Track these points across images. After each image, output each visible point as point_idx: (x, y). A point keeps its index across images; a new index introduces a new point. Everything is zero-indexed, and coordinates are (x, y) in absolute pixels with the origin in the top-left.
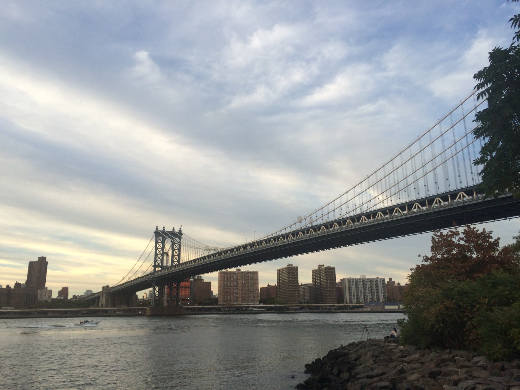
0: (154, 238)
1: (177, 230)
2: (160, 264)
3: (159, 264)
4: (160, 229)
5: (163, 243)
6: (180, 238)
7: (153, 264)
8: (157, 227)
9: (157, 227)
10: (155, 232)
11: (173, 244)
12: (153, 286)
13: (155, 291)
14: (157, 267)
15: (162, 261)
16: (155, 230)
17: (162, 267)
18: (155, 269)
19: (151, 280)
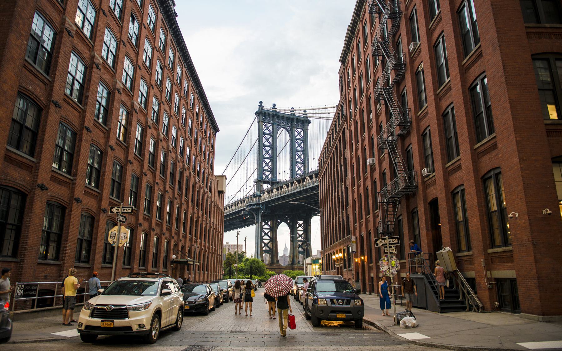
0: (256, 124)
1: (299, 113)
2: (270, 176)
3: (267, 177)
4: (268, 106)
5: (274, 135)
6: (305, 130)
7: (255, 176)
8: (261, 103)
9: (261, 103)
10: (258, 114)
11: (293, 139)
12: (258, 222)
13: (261, 234)
14: (264, 182)
15: (273, 171)
16: (257, 109)
17: (273, 182)
18: (259, 188)
19: (254, 207)
